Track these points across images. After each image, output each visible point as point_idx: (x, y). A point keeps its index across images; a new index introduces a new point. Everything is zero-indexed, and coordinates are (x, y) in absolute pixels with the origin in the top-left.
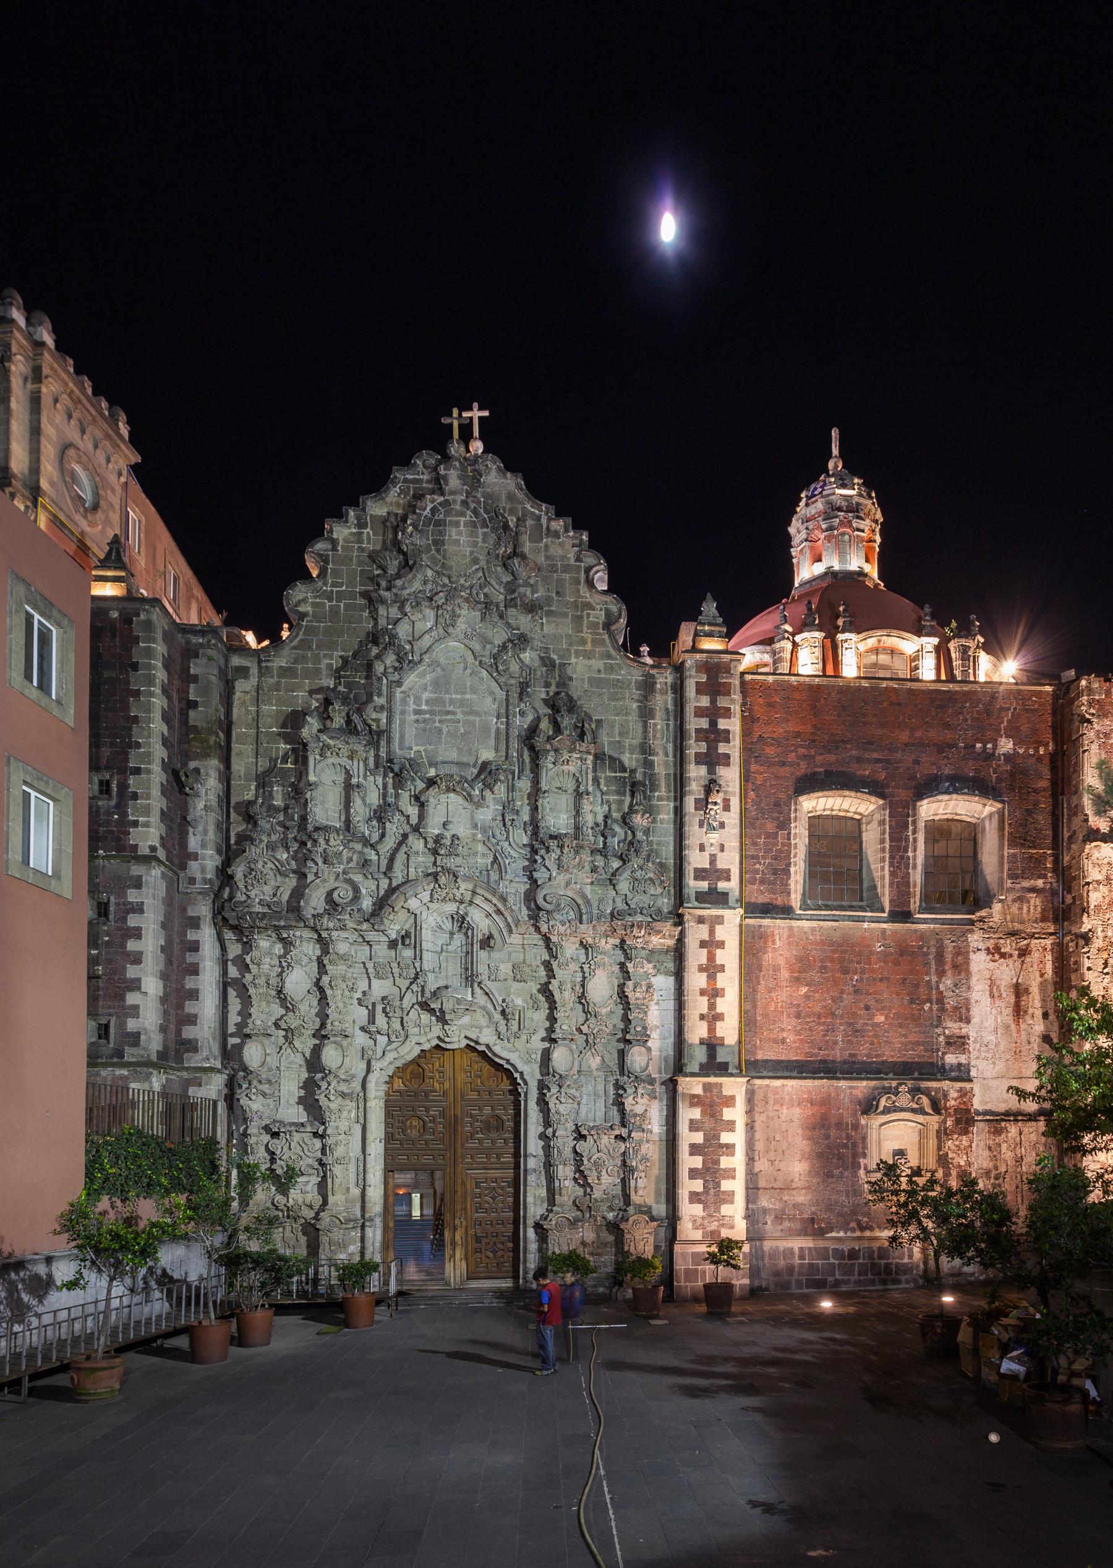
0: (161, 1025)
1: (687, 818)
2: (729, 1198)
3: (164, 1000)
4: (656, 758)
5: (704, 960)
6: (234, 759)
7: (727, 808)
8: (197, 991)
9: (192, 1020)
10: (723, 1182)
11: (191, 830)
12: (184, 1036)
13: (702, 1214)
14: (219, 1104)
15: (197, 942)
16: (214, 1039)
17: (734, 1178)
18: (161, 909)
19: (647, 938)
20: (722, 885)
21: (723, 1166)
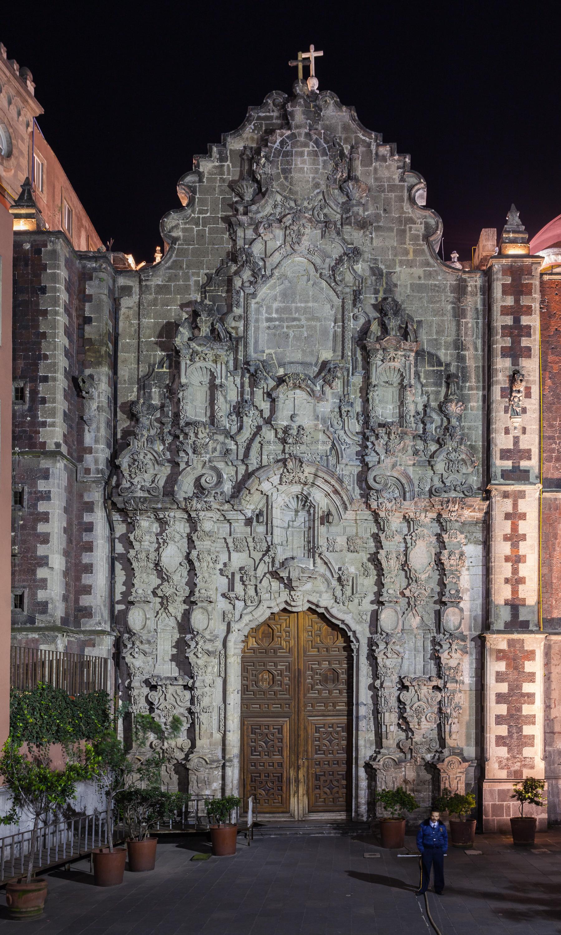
0: (64, 595)
1: (494, 405)
2: (530, 741)
3: (66, 574)
4: (467, 353)
5: (508, 531)
6: (120, 365)
7: (528, 395)
8: (91, 565)
9: (87, 590)
10: (524, 727)
11: (86, 428)
12: (81, 604)
13: (507, 755)
14: (109, 661)
15: (91, 524)
16: (105, 606)
17: (534, 723)
18: (64, 495)
19: (460, 512)
20: (524, 464)
21: (524, 712)
